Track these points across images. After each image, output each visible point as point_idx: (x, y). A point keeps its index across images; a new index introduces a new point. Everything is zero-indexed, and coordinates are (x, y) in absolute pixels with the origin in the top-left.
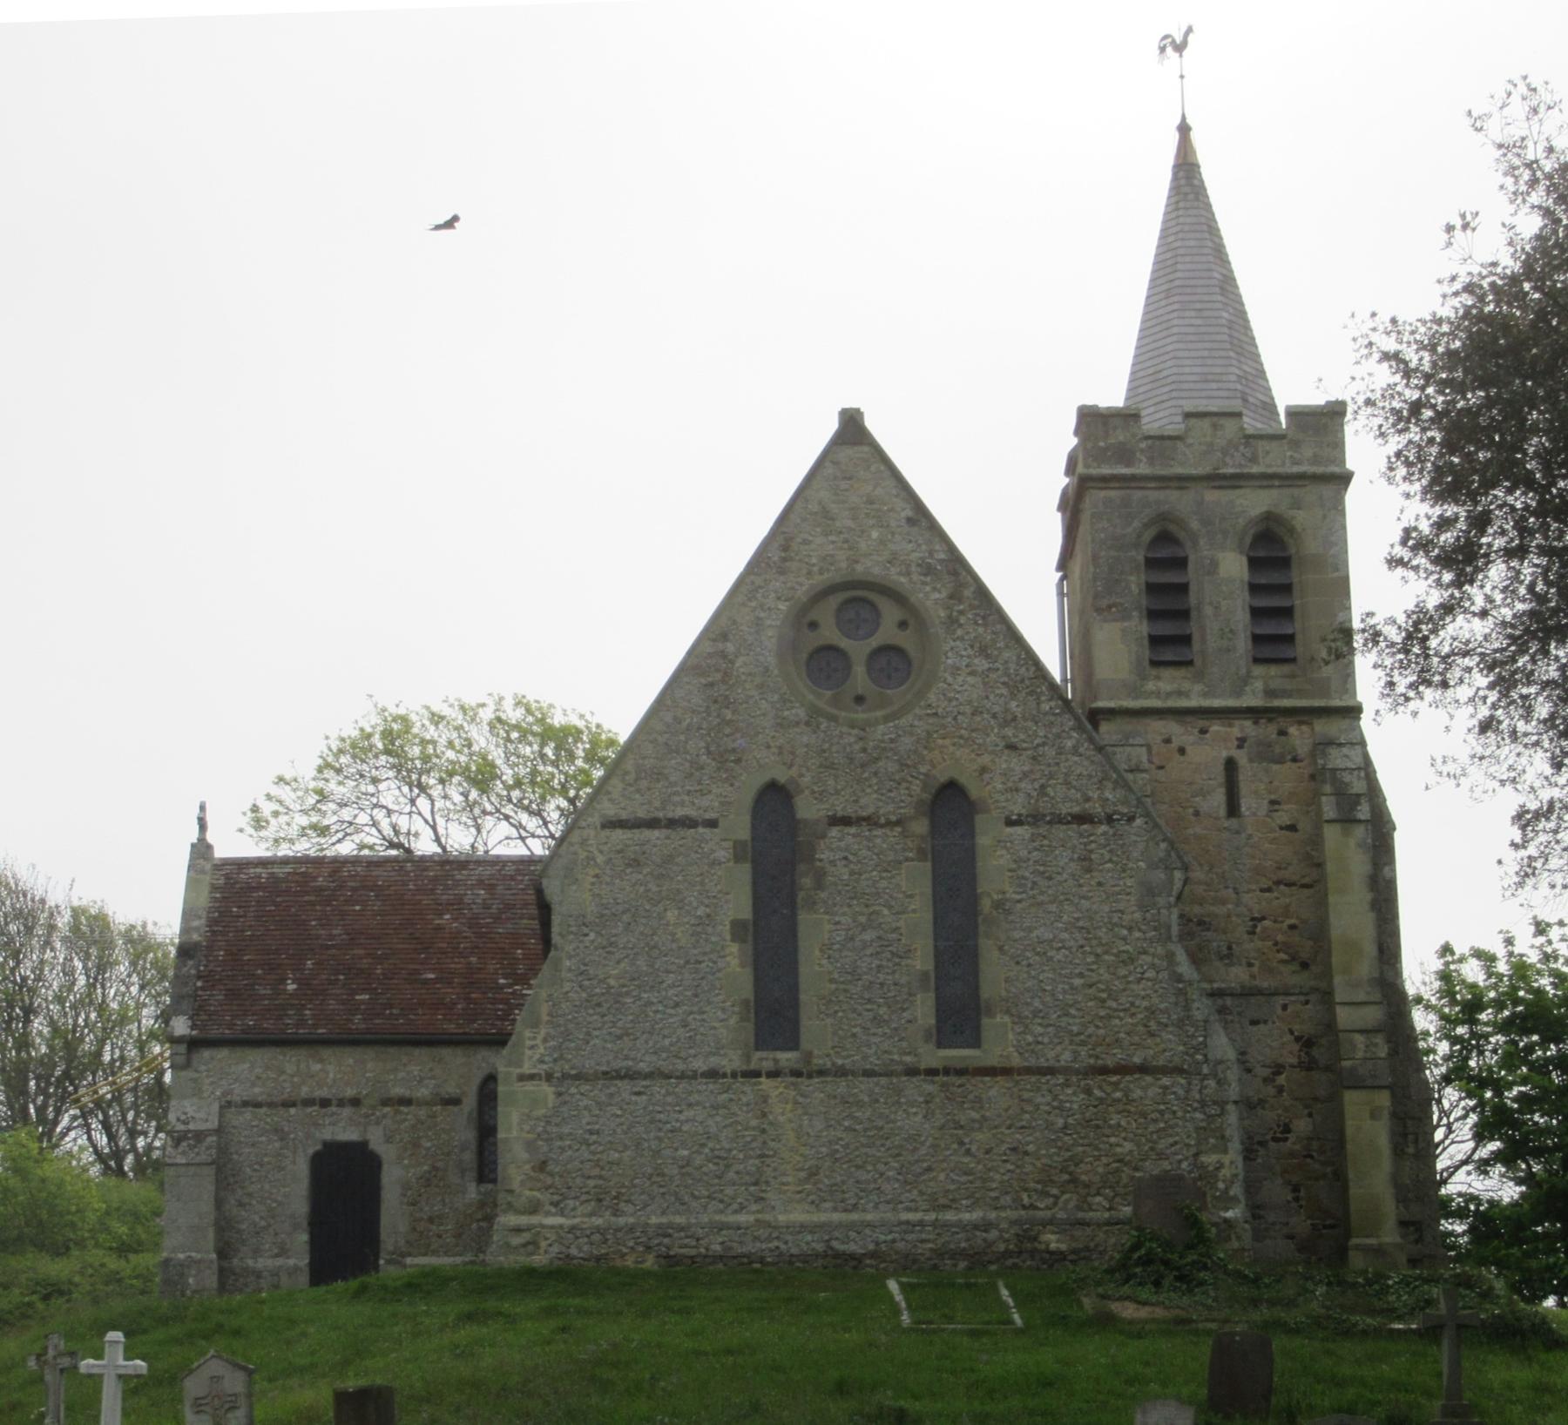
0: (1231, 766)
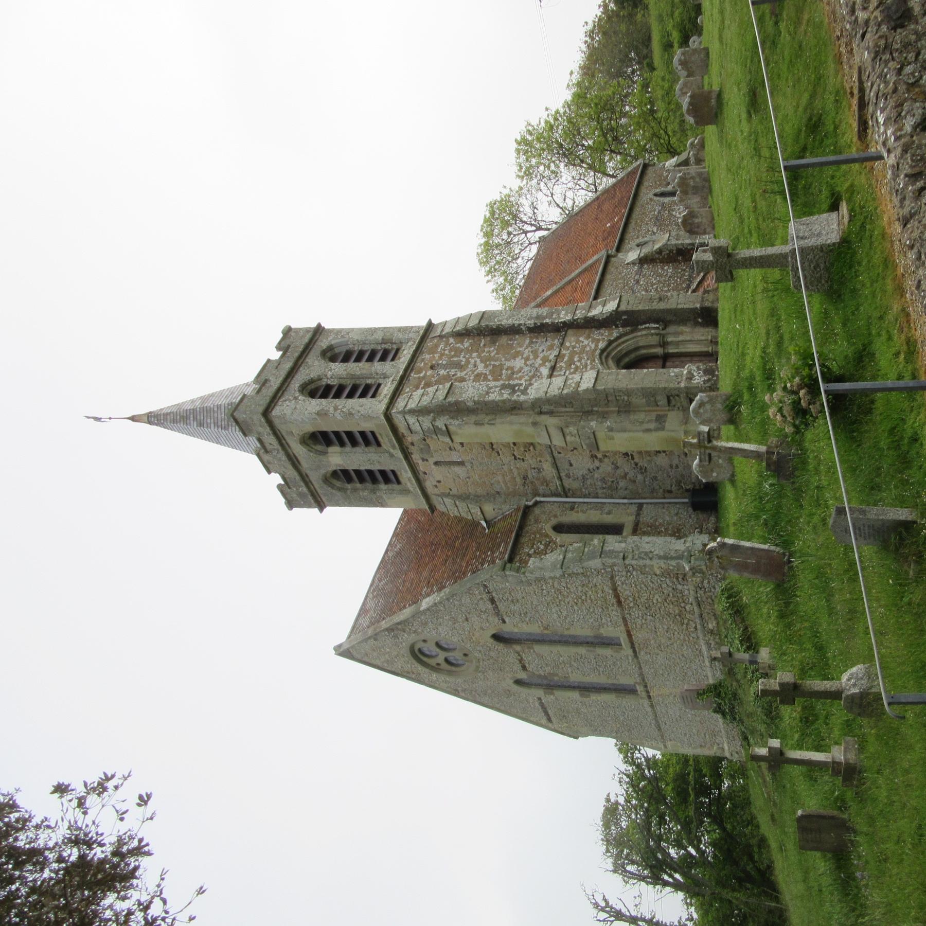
0: (436, 463)
